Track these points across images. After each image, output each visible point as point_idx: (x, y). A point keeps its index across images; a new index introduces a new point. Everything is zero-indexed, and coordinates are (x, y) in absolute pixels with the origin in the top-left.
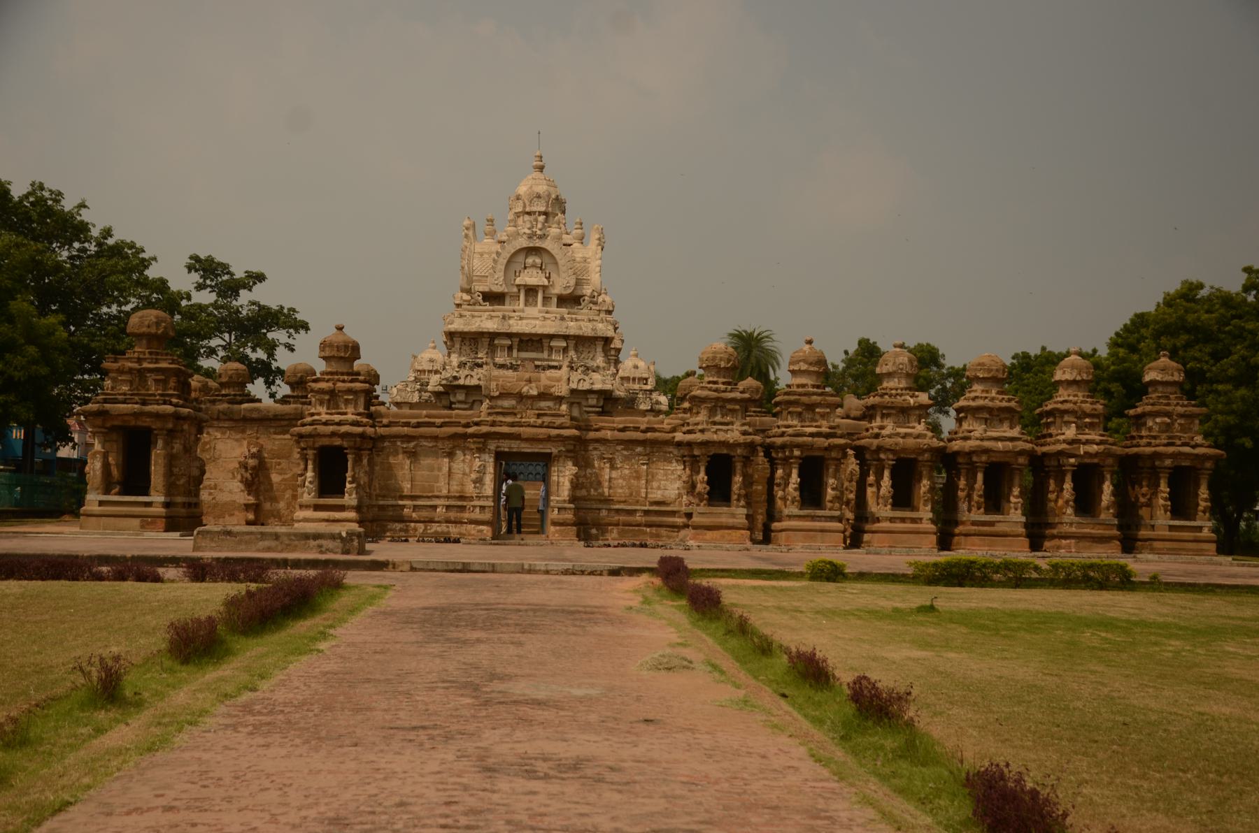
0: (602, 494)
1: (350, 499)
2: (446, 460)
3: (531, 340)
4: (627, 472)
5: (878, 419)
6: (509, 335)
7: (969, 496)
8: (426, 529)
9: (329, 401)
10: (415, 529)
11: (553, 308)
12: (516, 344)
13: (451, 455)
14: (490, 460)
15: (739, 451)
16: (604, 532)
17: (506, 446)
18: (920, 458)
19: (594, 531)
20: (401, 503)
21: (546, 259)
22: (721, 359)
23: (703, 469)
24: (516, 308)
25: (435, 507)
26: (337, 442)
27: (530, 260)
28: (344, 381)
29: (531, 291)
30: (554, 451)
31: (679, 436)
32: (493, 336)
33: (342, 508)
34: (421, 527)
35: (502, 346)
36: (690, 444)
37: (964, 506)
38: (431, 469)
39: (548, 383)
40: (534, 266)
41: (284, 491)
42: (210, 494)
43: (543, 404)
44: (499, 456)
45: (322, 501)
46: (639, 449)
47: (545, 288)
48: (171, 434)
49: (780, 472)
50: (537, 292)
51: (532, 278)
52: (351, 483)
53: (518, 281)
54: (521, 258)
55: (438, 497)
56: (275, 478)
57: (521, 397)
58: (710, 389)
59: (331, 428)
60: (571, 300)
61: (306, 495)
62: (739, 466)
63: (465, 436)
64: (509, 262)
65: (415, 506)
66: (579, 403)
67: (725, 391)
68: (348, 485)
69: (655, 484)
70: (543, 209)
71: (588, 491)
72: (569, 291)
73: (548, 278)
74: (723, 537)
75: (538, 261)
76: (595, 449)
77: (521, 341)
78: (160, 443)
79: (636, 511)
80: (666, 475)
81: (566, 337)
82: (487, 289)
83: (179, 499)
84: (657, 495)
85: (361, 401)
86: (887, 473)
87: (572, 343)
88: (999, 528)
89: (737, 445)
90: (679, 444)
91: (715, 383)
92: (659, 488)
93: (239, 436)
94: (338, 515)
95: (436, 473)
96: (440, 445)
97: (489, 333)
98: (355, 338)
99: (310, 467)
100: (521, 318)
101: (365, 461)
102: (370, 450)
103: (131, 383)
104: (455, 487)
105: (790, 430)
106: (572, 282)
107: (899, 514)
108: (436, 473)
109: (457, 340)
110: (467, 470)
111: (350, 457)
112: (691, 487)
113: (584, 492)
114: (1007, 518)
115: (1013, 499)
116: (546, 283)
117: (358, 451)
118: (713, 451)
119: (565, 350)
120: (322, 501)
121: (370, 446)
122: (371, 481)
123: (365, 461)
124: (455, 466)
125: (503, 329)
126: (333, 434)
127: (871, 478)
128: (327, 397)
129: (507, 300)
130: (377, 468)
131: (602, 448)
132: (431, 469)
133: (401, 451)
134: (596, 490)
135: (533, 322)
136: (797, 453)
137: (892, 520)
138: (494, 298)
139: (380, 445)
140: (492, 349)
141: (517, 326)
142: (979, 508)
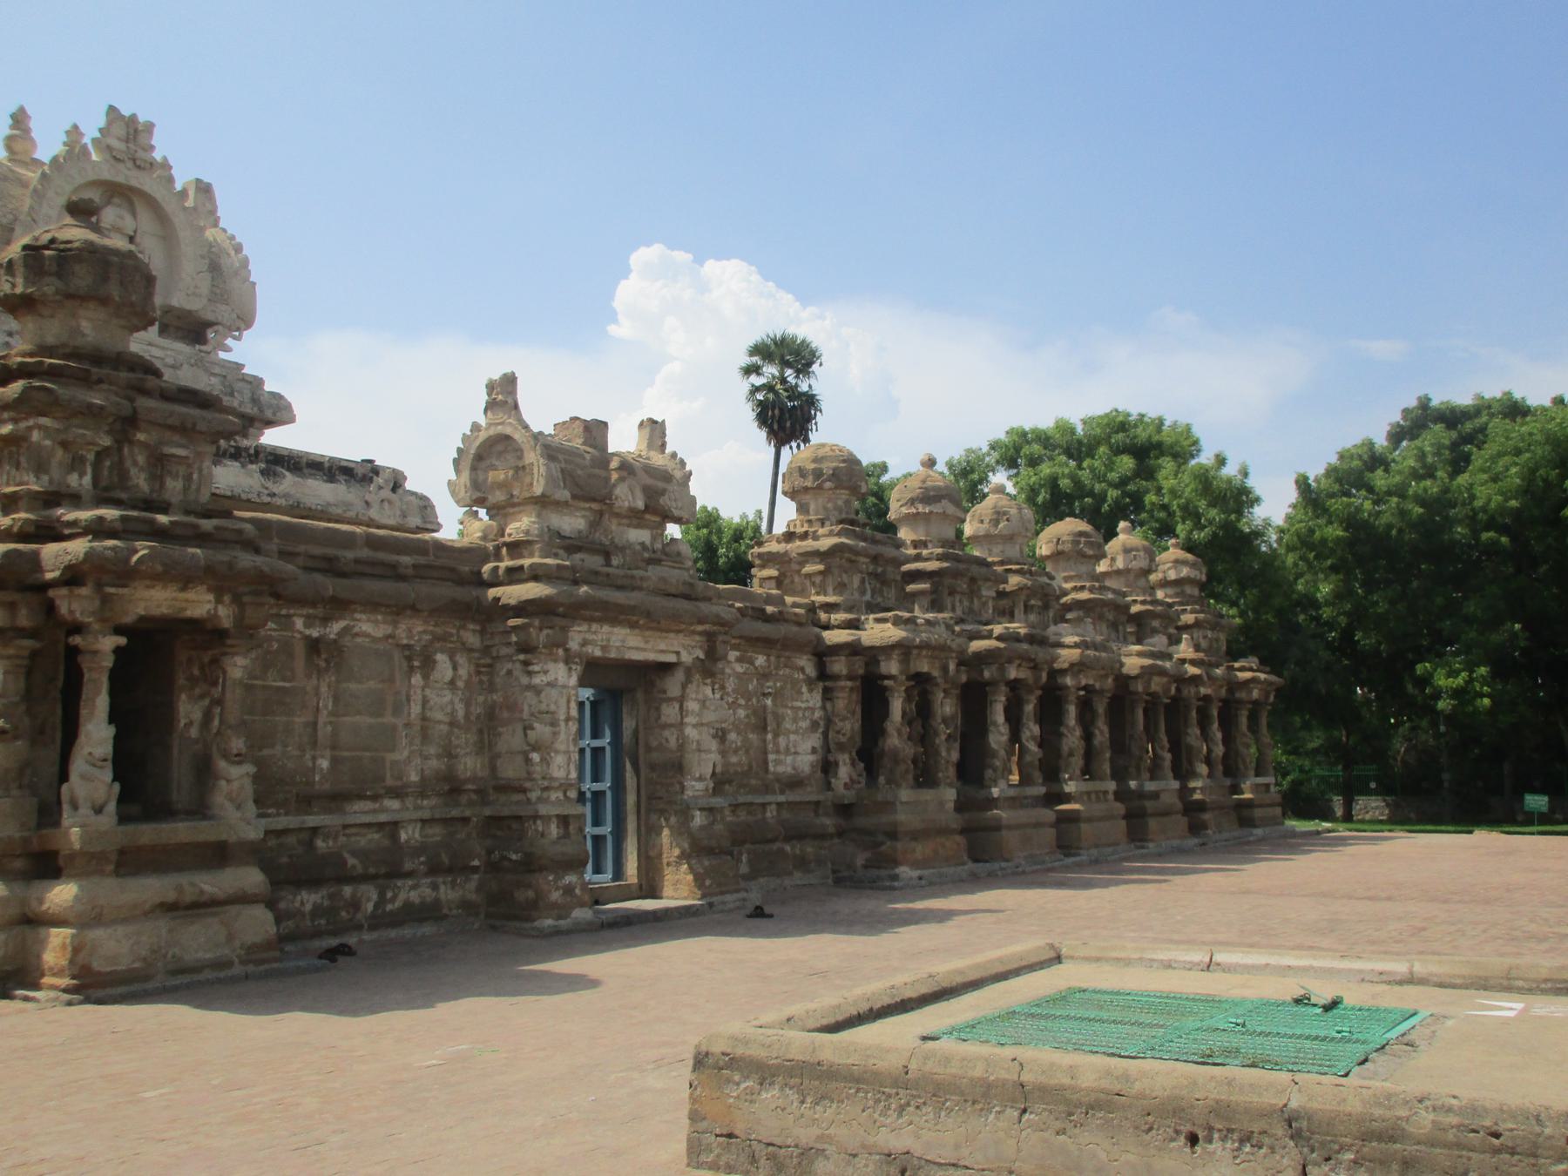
1: (236, 813)
4: (742, 713)
8: (382, 895)
10: (355, 905)
13: (428, 664)
18: (1097, 686)
20: (312, 821)
25: (393, 827)
26: (200, 603)
33: (219, 855)
34: (369, 896)
46: (760, 660)
55: (397, 793)
69: (782, 741)
80: (795, 720)
95: (388, 719)
124: (434, 699)
128: (106, 441)
133: (300, 650)
136: (1013, 673)
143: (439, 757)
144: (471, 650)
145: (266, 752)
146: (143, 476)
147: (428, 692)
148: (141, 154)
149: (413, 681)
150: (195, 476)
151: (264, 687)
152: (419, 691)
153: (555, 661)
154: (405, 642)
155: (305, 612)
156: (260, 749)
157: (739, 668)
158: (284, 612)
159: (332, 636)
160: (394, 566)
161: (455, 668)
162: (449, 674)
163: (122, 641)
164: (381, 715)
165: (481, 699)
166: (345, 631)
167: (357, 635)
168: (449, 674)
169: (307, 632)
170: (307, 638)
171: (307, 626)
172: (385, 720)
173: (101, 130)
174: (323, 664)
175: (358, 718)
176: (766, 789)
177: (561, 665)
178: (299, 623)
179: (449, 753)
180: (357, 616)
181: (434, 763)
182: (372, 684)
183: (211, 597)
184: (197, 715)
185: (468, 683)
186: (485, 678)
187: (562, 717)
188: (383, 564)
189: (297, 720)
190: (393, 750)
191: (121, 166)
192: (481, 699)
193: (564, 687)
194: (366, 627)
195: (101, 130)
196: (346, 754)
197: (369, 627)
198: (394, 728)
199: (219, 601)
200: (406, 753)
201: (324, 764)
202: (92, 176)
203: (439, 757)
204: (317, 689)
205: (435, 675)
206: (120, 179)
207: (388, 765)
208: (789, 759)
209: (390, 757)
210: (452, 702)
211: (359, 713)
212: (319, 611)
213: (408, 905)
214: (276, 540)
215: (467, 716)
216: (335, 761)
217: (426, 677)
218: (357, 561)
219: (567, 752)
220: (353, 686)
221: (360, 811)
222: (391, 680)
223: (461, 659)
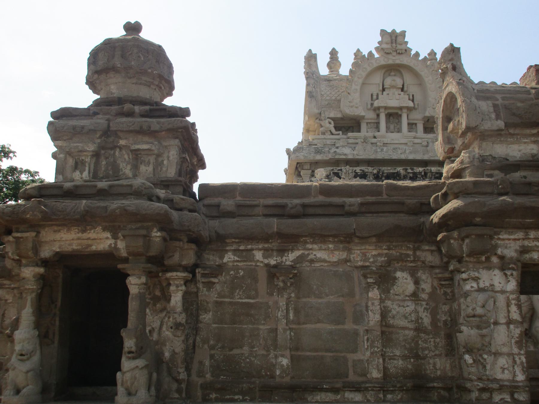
13: (384, 279)
21: (409, 79)
24: (377, 134)
26: (101, 240)
29: (394, 116)
38: (338, 315)
40: (393, 87)
47: (409, 109)
51: (393, 99)
52: (137, 354)
53: (376, 104)
64: (363, 84)
68: (126, 364)
73: (413, 101)
82: (339, 115)
95: (349, 326)
101: (176, 299)
102: (192, 269)
104: (398, 365)
111: (135, 284)
116: (411, 104)
117: (157, 265)
121: (190, 259)
122: (191, 350)
123: (176, 299)
124: (394, 308)
129: (364, 126)
130: (206, 317)
135: (400, 146)
138: (348, 125)
143: (405, 358)
144: (432, 267)
145: (236, 351)
146: (129, 167)
147: (388, 303)
148: (399, 47)
149: (370, 294)
150: (165, 162)
151: (231, 303)
152: (377, 303)
153: (489, 268)
154: (360, 264)
155: (260, 246)
156: (231, 350)
158: (242, 248)
159: (288, 263)
160: (342, 206)
161: (417, 282)
162: (411, 288)
163: (42, 270)
164: (343, 323)
165: (446, 308)
167: (312, 261)
168: (411, 288)
169: (266, 261)
170: (267, 265)
171: (265, 257)
172: (346, 327)
173: (379, 43)
174: (281, 284)
175: (319, 326)
177: (497, 272)
178: (258, 255)
179: (415, 354)
180: (309, 246)
181: (400, 363)
182: (332, 299)
183: (109, 235)
184: (156, 325)
185: (432, 295)
186: (449, 291)
187: (503, 321)
188: (330, 205)
189: (261, 327)
191: (390, 56)
192: (446, 308)
193: (503, 292)
194: (321, 255)
195: (379, 43)
196: (308, 354)
197: (324, 254)
198: (356, 333)
199: (115, 237)
200: (368, 353)
201: (285, 362)
202: (375, 65)
203: (405, 358)
204: (276, 303)
205: (396, 289)
206: (390, 62)
207: (350, 364)
209: (352, 357)
210: (416, 311)
211: (319, 321)
212: (274, 244)
214: (239, 198)
215: (434, 322)
217: (385, 291)
218: (304, 206)
219: (510, 355)
220: (313, 300)
222: (351, 294)
223: (423, 275)
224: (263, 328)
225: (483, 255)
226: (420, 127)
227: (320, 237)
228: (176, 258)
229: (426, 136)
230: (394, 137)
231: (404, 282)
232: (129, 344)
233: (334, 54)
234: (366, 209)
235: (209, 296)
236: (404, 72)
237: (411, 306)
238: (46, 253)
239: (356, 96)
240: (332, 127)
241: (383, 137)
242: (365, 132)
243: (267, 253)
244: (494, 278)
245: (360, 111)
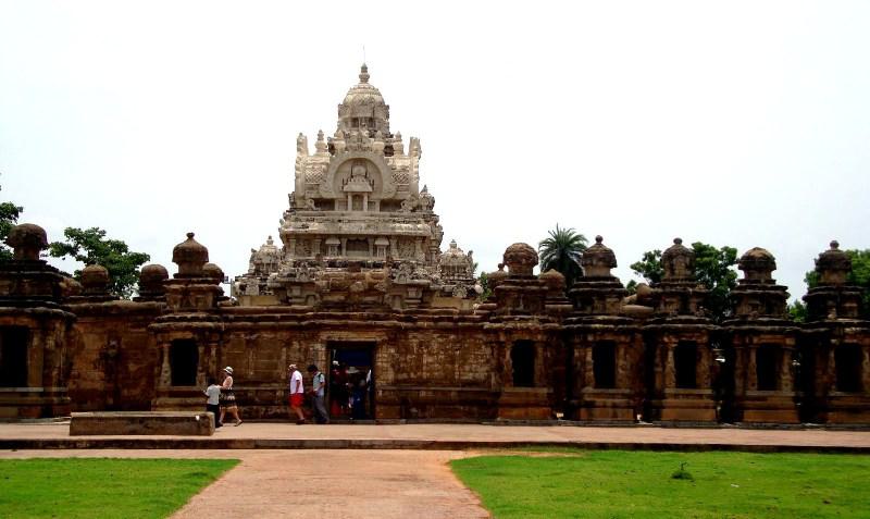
0: (421, 377)
2: (284, 349)
3: (358, 240)
5: (662, 306)
6: (339, 237)
7: (744, 376)
9: (182, 300)
10: (257, 411)
11: (377, 211)
12: (344, 245)
13: (288, 344)
14: (320, 348)
15: (539, 337)
16: (424, 410)
17: (336, 336)
19: (414, 410)
21: (370, 169)
22: (523, 257)
23: (508, 353)
25: (274, 391)
26: (189, 335)
27: (356, 170)
28: (194, 282)
29: (358, 196)
30: (378, 340)
31: (487, 325)
32: (324, 237)
35: (333, 246)
36: (496, 331)
37: (739, 383)
38: (270, 357)
39: (373, 281)
41: (140, 377)
42: (74, 383)
43: (369, 299)
44: (330, 345)
45: (176, 388)
46: (452, 337)
48: (46, 331)
49: (576, 354)
50: (363, 197)
51: (358, 186)
52: (201, 371)
54: (347, 168)
55: (275, 382)
56: (132, 367)
57: (349, 293)
58: (514, 283)
59: (185, 324)
60: (391, 204)
61: (162, 383)
62: (540, 350)
63: (301, 328)
64: (337, 172)
65: (257, 391)
66: (400, 296)
67: (528, 284)
68: (200, 374)
69: (467, 368)
70: (369, 115)
71: (409, 375)
72: (390, 196)
74: (527, 414)
75: (363, 170)
76: (414, 337)
77: (349, 240)
78: (36, 342)
79: (450, 391)
80: (476, 358)
81: (388, 237)
83: (54, 389)
84: (470, 376)
85: (210, 298)
86: (671, 354)
87: (394, 243)
88: (770, 402)
89: (537, 331)
90: (488, 332)
91: (516, 277)
92: (471, 371)
93: (99, 330)
94: (190, 400)
95: (275, 361)
96: (278, 335)
97: (321, 235)
98: (206, 246)
99: (166, 358)
100: (349, 221)
101: (213, 352)
103: (10, 287)
105: (584, 318)
106: (394, 189)
107: (681, 391)
108: (275, 361)
109: (293, 241)
110: (303, 358)
111: (201, 349)
112: (499, 368)
113: (405, 376)
114: (779, 393)
115: (784, 378)
116: (370, 189)
118: (516, 337)
119: (388, 248)
120: (176, 388)
123: (213, 352)
124: (292, 355)
125: (332, 231)
126: (188, 328)
127: (657, 360)
128: (180, 296)
129: (337, 205)
131: (420, 336)
132: (270, 357)
134: (415, 373)
137: (676, 396)
138: (324, 204)
139: (225, 336)
140: (324, 249)
141: (346, 229)
142: (753, 385)
157: (440, 340)
166: (258, 337)
176: (452, 385)
178: (243, 336)
190: (276, 368)
197: (267, 335)
208: (471, 374)
213: (276, 413)
216: (256, 373)
221: (262, 388)
224: (245, 361)
225: (314, 338)
226: (378, 204)
227: (266, 329)
228: (213, 339)
229: (382, 213)
230: (357, 215)
231: (296, 345)
232: (200, 368)
233: (320, 136)
234: (283, 318)
235: (224, 350)
236: (368, 164)
237: (297, 354)
238: (171, 339)
239: (330, 183)
240: (313, 205)
241: (349, 215)
242: (338, 210)
243: (246, 335)
244: (318, 346)
245: (333, 195)
